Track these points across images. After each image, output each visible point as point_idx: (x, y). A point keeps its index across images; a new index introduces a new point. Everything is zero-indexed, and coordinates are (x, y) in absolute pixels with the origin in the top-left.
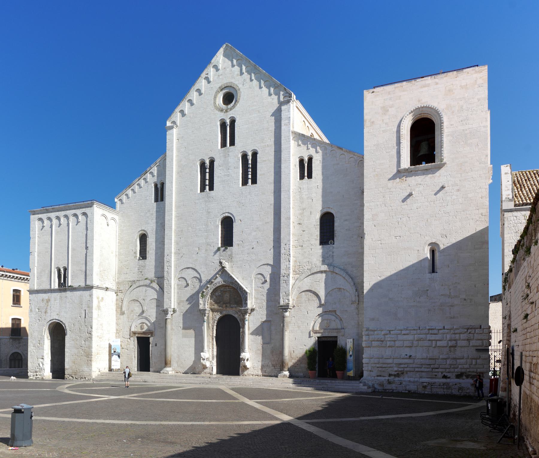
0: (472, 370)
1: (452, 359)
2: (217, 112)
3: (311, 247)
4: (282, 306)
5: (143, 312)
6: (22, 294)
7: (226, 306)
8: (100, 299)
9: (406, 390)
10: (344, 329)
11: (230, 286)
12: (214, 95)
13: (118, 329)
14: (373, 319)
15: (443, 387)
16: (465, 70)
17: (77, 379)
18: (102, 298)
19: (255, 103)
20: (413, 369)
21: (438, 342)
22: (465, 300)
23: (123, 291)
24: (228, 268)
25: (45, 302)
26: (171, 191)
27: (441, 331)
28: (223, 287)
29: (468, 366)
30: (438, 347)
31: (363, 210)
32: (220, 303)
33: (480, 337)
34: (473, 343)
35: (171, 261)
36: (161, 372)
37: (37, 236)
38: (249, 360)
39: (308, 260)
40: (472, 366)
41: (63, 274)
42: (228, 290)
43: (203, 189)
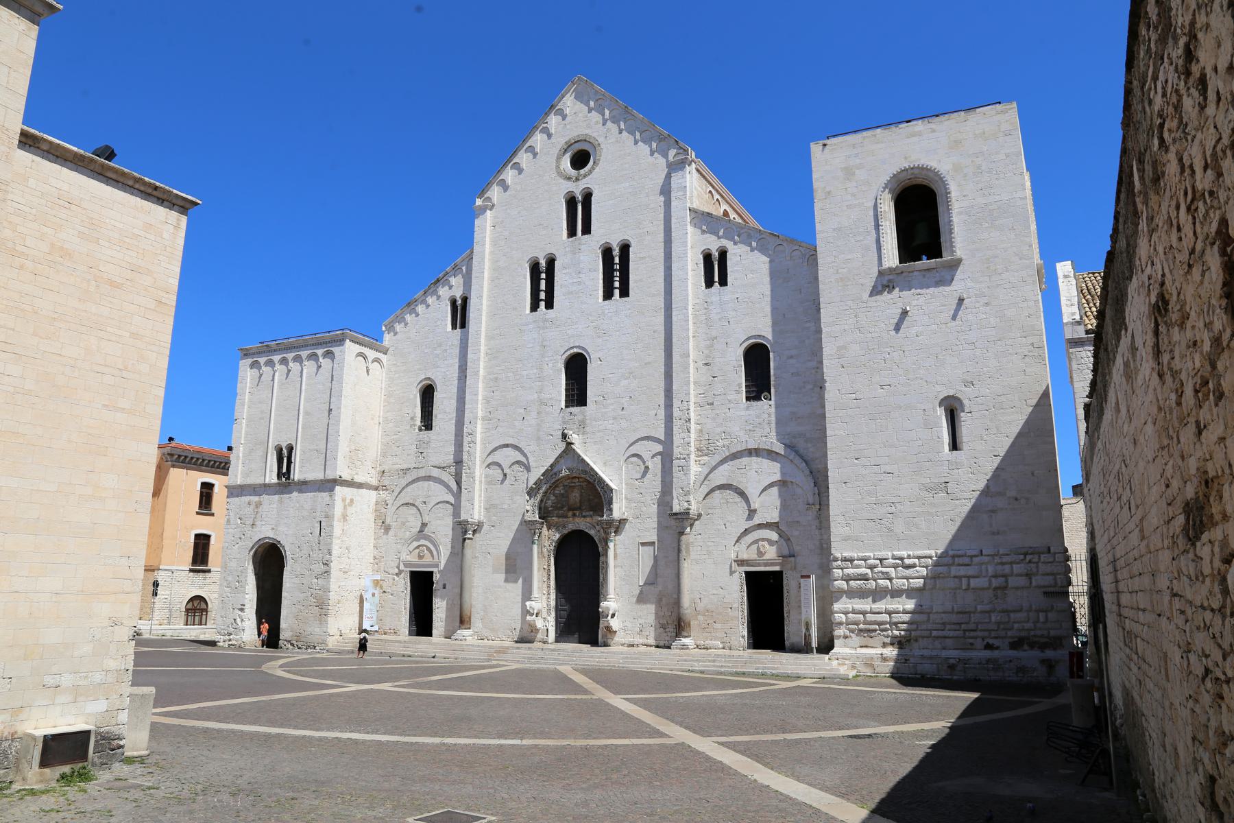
0: (1039, 633)
1: (1000, 612)
2: (562, 181)
3: (729, 406)
4: (676, 514)
5: (424, 525)
6: (216, 489)
7: (574, 515)
8: (348, 501)
9: (916, 674)
10: (794, 556)
11: (581, 478)
12: (556, 155)
13: (377, 557)
14: (846, 539)
15: (985, 666)
16: (978, 110)
17: (299, 648)
18: (352, 500)
19: (627, 166)
20: (929, 632)
21: (972, 581)
22: (1016, 499)
23: (388, 487)
24: (578, 448)
25: (252, 507)
26: (480, 310)
27: (976, 560)
28: (569, 479)
29: (1032, 625)
30: (973, 589)
31: (820, 340)
32: (562, 508)
33: (1049, 568)
34: (1036, 581)
35: (476, 432)
36: (452, 637)
37: (248, 391)
38: (616, 615)
39: (724, 429)
40: (1039, 625)
41: (285, 457)
42: (577, 484)
43: (534, 307)
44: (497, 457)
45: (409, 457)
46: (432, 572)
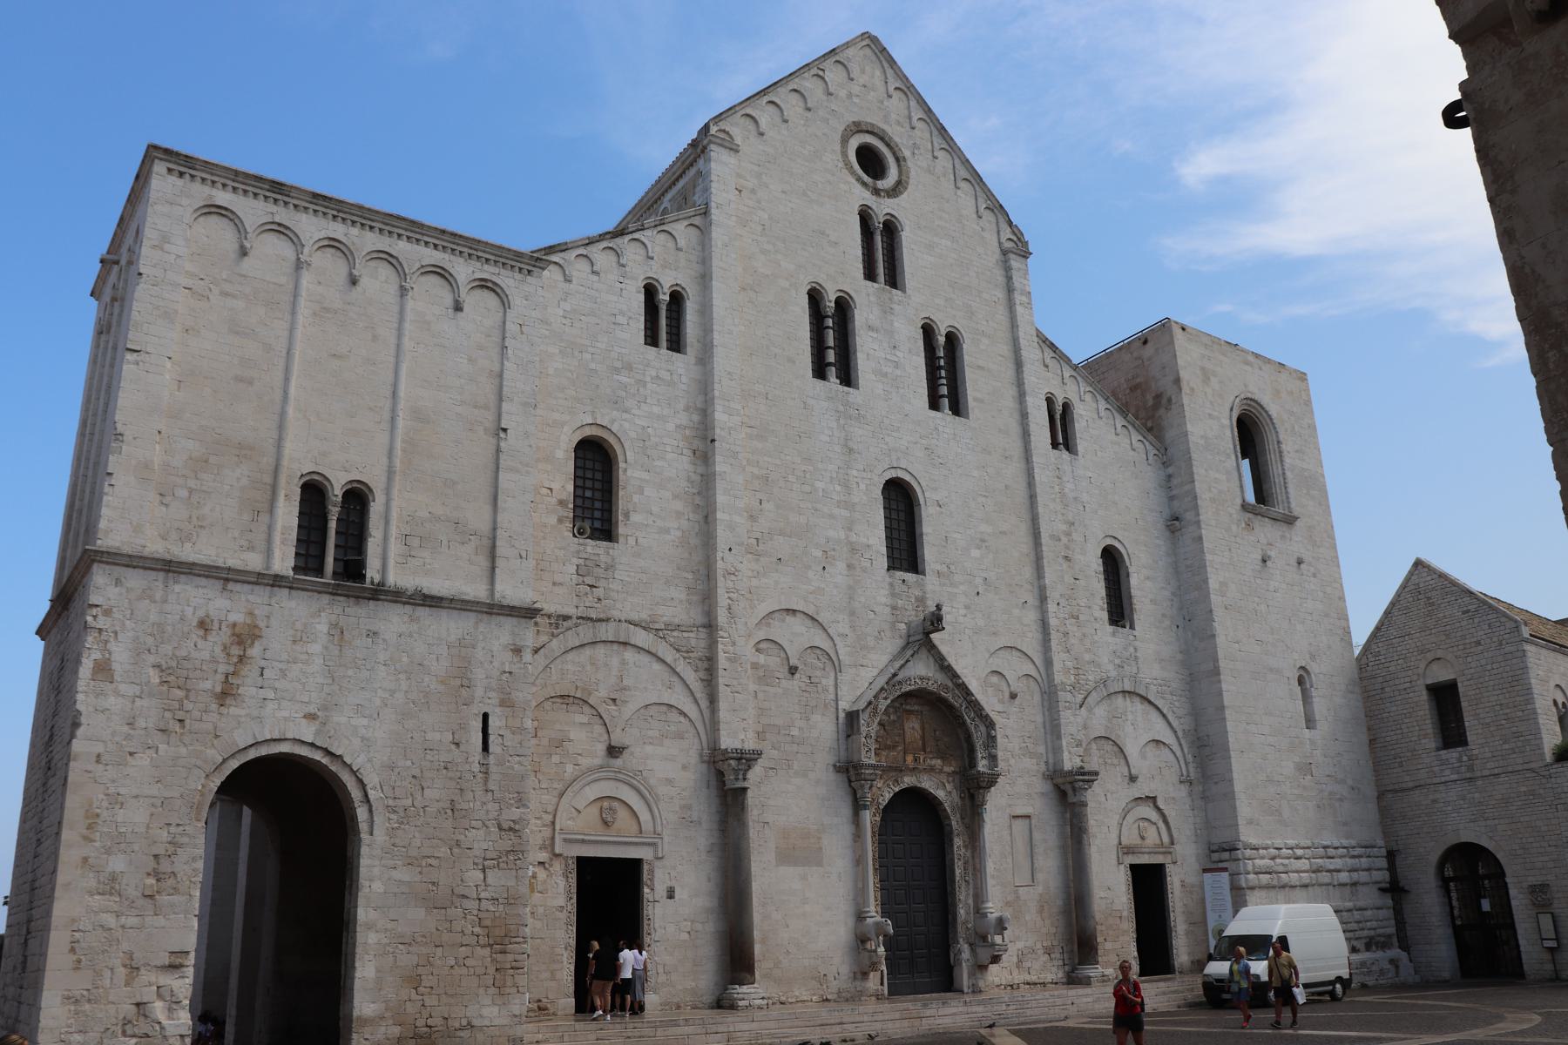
2: (854, 181)
32: (893, 747)
44: (778, 631)
45: (556, 589)
46: (637, 863)
